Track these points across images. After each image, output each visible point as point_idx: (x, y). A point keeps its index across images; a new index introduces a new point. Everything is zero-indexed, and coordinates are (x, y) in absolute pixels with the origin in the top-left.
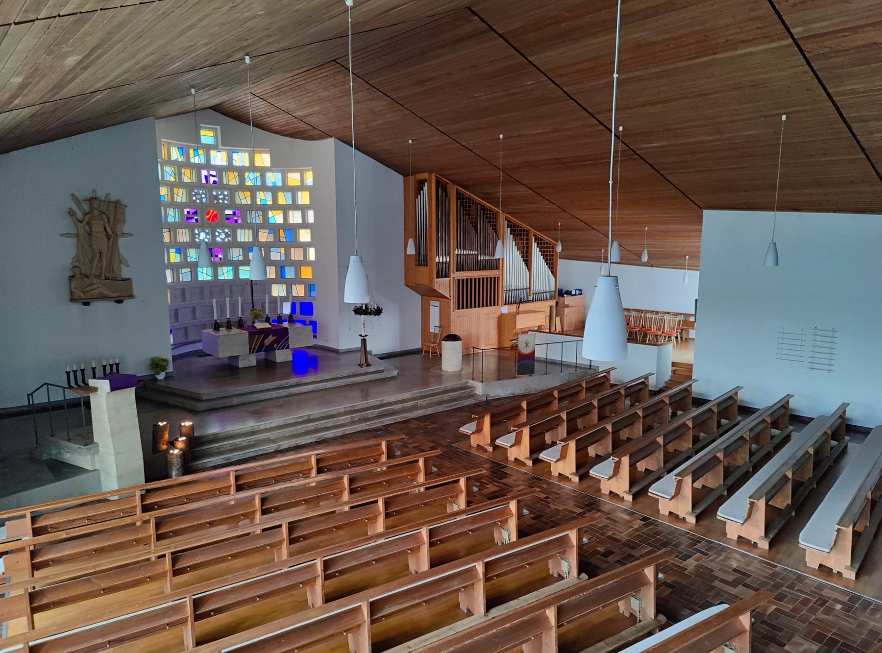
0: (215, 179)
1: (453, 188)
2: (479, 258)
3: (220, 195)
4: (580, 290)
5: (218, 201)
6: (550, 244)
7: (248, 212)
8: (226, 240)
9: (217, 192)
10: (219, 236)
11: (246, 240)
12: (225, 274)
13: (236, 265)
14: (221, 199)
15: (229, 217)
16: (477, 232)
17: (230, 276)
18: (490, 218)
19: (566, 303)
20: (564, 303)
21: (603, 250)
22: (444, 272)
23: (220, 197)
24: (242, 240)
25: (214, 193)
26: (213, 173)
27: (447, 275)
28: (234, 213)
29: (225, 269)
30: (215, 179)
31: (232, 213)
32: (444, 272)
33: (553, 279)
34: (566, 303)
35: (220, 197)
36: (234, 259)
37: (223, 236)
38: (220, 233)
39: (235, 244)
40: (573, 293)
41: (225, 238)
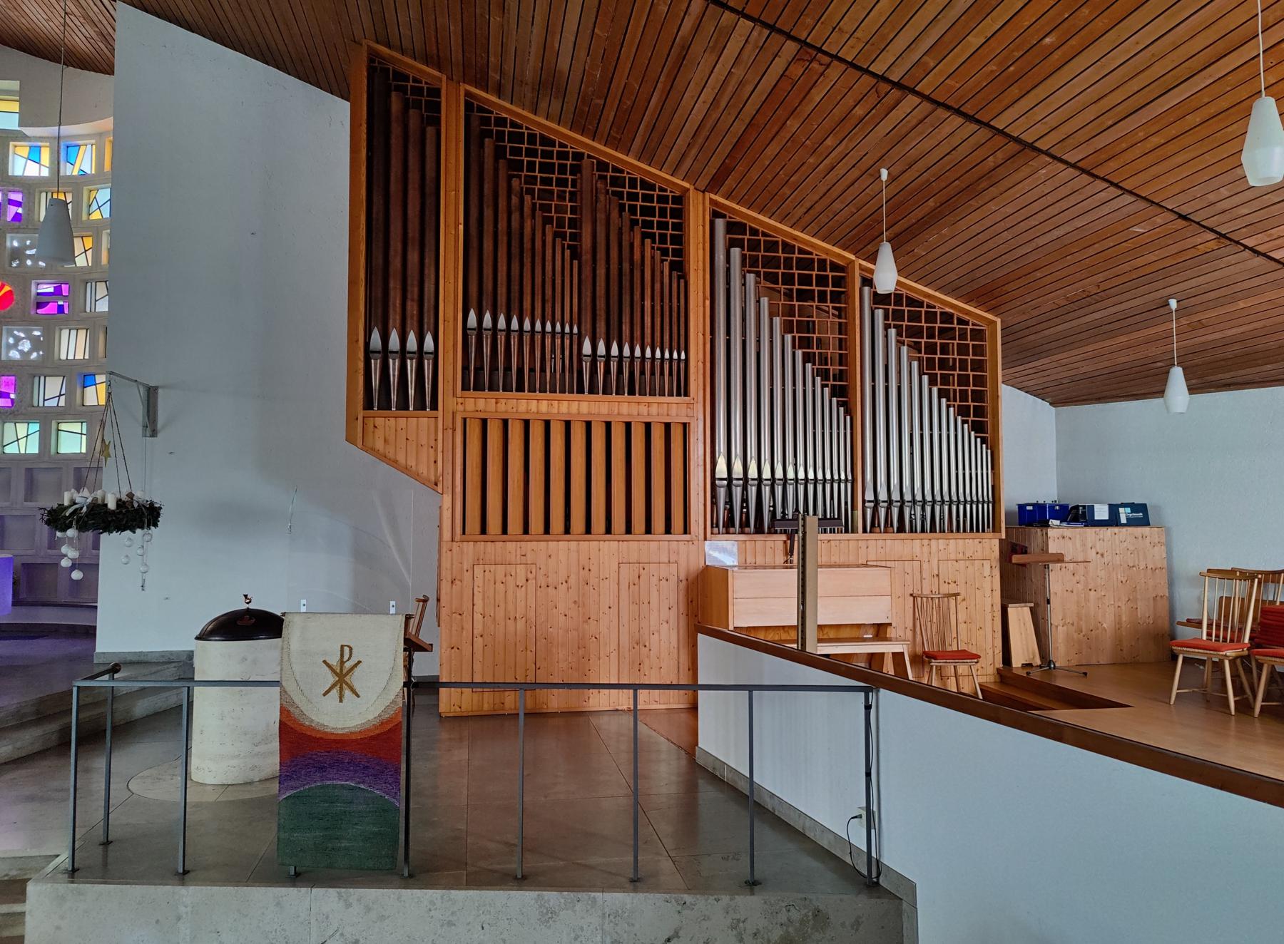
0: (20, 210)
1: (458, 95)
2: (587, 348)
3: (30, 248)
4: (1142, 508)
5: (22, 264)
6: (961, 321)
7: (89, 285)
8: (34, 355)
9: (22, 241)
10: (15, 346)
11: (79, 356)
12: (22, 442)
13: (48, 420)
14: (30, 257)
15: (45, 299)
16: (576, 254)
17: (33, 448)
18: (648, 211)
19: (1053, 548)
20: (1045, 549)
21: (1173, 304)
22: (411, 392)
23: (28, 252)
24: (71, 357)
25: (16, 244)
26: (17, 197)
27: (427, 401)
28: (58, 291)
29: (22, 429)
30: (20, 210)
31: (51, 290)
32: (411, 392)
33: (986, 451)
34: (1053, 548)
35: (28, 252)
36: (47, 404)
37: (26, 346)
38: (18, 339)
39: (50, 365)
40: (1102, 513)
41: (30, 352)
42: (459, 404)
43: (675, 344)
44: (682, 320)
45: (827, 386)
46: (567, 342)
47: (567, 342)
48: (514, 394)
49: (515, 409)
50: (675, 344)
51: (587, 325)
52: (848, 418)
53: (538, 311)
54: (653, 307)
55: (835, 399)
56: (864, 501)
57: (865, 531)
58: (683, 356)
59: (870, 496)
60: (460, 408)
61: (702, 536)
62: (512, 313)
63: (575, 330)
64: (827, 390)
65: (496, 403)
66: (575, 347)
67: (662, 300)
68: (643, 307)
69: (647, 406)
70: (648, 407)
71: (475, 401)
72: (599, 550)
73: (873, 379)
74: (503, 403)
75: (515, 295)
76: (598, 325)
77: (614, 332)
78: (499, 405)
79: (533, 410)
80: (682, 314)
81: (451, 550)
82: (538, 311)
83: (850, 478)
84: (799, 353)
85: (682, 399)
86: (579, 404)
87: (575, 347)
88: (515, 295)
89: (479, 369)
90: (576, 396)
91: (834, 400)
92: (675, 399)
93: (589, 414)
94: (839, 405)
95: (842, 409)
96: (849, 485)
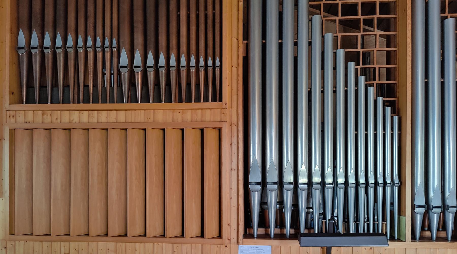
2: (124, 60)
42: (11, 117)
43: (210, 51)
44: (217, 26)
45: (370, 85)
46: (108, 55)
47: (108, 55)
48: (61, 106)
49: (59, 121)
50: (210, 51)
51: (126, 38)
52: (396, 118)
53: (81, 28)
54: (188, 17)
55: (381, 98)
56: (413, 207)
57: (413, 238)
58: (218, 63)
59: (420, 200)
60: (12, 120)
61: (234, 240)
62: (57, 31)
63: (115, 43)
64: (371, 90)
65: (43, 115)
66: (115, 60)
67: (197, 9)
68: (178, 16)
69: (181, 113)
70: (183, 114)
71: (24, 114)
72: (136, 250)
73: (426, 75)
74: (49, 115)
75: (61, 13)
76: (135, 37)
77: (151, 44)
78: (45, 116)
79: (74, 122)
80: (217, 21)
81: (6, 248)
82: (81, 28)
83: (396, 181)
84: (341, 52)
85: (217, 104)
86: (117, 114)
87: (115, 60)
88: (61, 13)
89: (30, 86)
90: (116, 106)
91: (380, 100)
92: (210, 104)
93: (127, 122)
94: (385, 105)
95: (389, 109)
96: (396, 189)
